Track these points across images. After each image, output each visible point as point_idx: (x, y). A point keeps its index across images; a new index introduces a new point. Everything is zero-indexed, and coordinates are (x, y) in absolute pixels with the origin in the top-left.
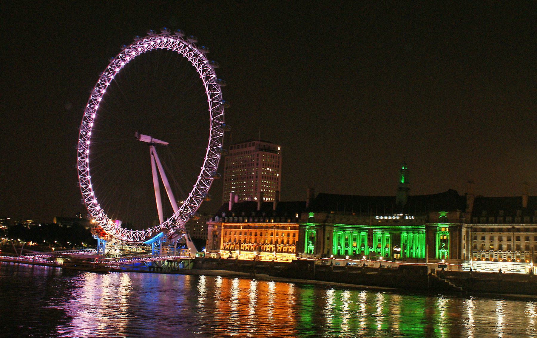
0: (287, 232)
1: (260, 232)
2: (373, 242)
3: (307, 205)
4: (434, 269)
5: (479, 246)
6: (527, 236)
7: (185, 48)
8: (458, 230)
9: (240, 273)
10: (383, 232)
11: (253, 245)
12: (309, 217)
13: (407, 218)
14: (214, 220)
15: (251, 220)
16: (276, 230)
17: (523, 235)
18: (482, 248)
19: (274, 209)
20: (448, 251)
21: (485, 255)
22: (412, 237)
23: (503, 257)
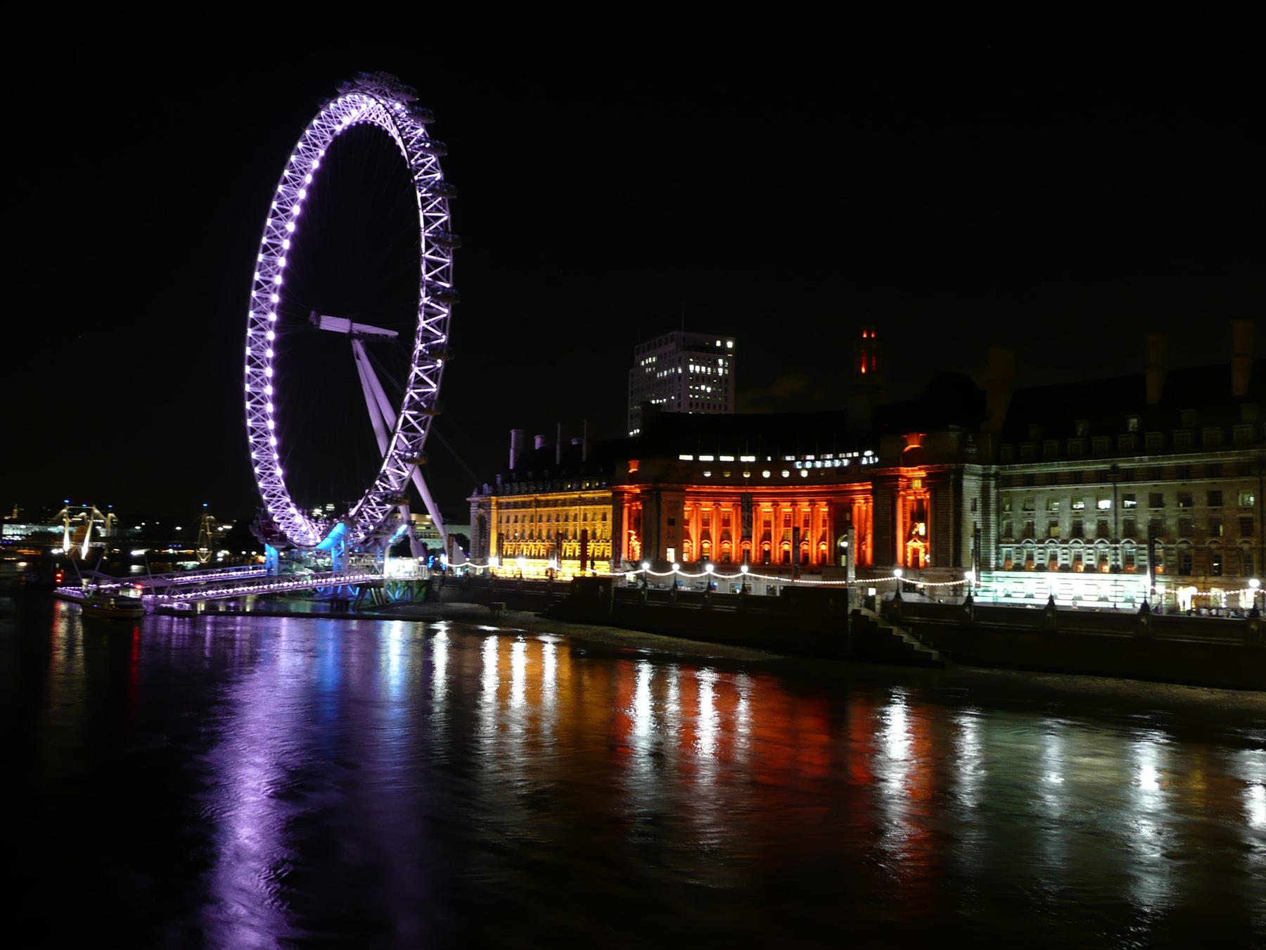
0: (602, 512)
1: (555, 515)
2: (752, 527)
5: (1018, 528)
6: (1155, 491)
8: (951, 483)
10: (813, 501)
11: (543, 543)
12: (631, 471)
13: (864, 462)
14: (480, 493)
16: (582, 507)
18: (1029, 532)
20: (928, 544)
21: (1035, 554)
23: (1085, 558)
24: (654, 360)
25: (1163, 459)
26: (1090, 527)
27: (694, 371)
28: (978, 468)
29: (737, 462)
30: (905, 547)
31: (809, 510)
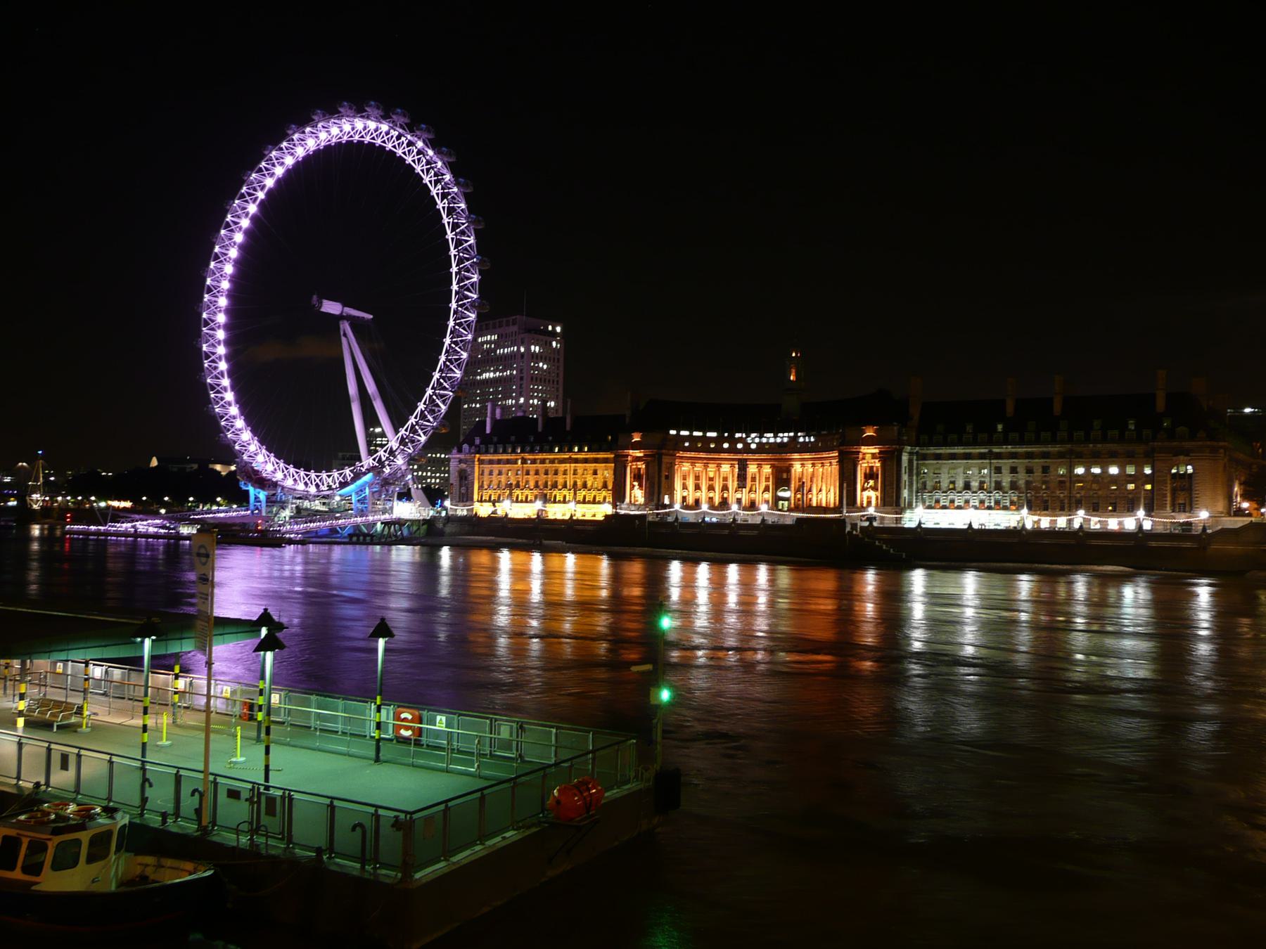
0: (593, 468)
1: (544, 470)
3: (627, 420)
4: (856, 524)
5: (929, 484)
6: (1013, 465)
7: (400, 139)
9: (509, 540)
12: (633, 441)
13: (801, 440)
14: (460, 451)
15: (528, 449)
16: (573, 465)
17: (1006, 464)
19: (568, 428)
20: (878, 493)
22: (810, 474)
24: (496, 338)
25: (1019, 448)
26: (975, 484)
27: (535, 350)
28: (909, 448)
29: (704, 436)
30: (861, 495)
31: (757, 470)
